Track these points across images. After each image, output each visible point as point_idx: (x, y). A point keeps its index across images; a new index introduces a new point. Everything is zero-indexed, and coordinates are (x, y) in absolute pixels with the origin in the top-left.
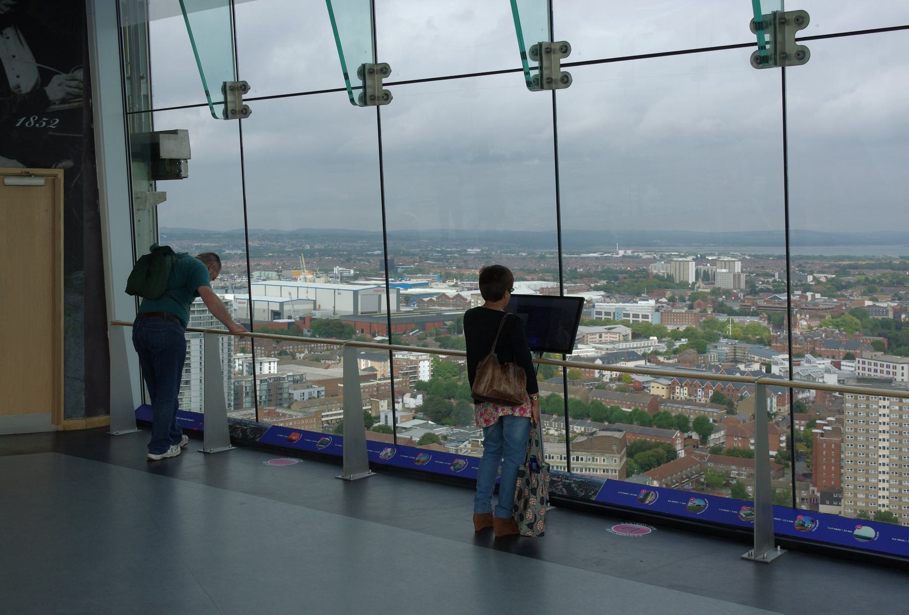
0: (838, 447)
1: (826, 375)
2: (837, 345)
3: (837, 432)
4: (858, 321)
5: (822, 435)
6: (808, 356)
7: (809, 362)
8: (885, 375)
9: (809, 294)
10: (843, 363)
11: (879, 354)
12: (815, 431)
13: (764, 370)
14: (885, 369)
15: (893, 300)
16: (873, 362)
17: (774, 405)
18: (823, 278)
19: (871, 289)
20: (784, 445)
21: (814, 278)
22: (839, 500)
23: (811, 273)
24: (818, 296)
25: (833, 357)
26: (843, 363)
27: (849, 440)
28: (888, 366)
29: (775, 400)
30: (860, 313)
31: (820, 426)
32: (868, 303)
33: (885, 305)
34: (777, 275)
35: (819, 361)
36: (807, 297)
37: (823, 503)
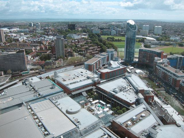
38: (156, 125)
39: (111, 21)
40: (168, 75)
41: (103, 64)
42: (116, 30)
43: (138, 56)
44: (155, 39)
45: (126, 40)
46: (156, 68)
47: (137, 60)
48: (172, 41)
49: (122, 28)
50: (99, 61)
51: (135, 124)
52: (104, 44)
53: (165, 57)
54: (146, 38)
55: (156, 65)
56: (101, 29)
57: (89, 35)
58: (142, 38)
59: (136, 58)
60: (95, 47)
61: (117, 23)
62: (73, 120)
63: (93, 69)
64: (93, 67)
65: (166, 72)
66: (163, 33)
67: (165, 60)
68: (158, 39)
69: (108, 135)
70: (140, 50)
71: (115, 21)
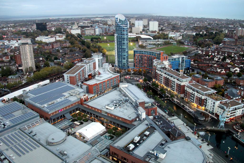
0: (20, 57)
1: (16, 44)
2: (17, 38)
3: (20, 54)
4: (20, 33)
5: (17, 55)
6: (12, 40)
7: (12, 41)
8: (26, 42)
9: (9, 28)
10: (18, 41)
11: (25, 38)
12: (15, 54)
13: (3, 44)
14: (26, 41)
15: (26, 28)
16: (24, 40)
17: (6, 51)
18: (11, 25)
19: (21, 26)
20: (10, 58)
21: (10, 25)
22: (22, 66)
23: (9, 24)
24: (11, 28)
25: (16, 40)
26: (18, 41)
27: (22, 55)
28: (27, 40)
29: (6, 50)
30: (20, 31)
31: (16, 53)
32: (21, 29)
33: (24, 29)
34: (2, 25)
35: (14, 41)
36: (9, 29)
37: (19, 67)
38: (164, 142)
39: (95, 16)
40: (171, 80)
41: (89, 74)
42: (101, 28)
43: (133, 60)
44: (151, 38)
45: (116, 40)
46: (156, 73)
48: (171, 38)
49: (110, 26)
50: (83, 70)
51: (138, 146)
52: (89, 47)
53: (166, 59)
54: (140, 37)
56: (82, 27)
58: (135, 36)
61: (103, 19)
62: (57, 153)
65: (168, 77)
66: (159, 30)
67: (166, 63)
70: (134, 51)
71: (99, 16)
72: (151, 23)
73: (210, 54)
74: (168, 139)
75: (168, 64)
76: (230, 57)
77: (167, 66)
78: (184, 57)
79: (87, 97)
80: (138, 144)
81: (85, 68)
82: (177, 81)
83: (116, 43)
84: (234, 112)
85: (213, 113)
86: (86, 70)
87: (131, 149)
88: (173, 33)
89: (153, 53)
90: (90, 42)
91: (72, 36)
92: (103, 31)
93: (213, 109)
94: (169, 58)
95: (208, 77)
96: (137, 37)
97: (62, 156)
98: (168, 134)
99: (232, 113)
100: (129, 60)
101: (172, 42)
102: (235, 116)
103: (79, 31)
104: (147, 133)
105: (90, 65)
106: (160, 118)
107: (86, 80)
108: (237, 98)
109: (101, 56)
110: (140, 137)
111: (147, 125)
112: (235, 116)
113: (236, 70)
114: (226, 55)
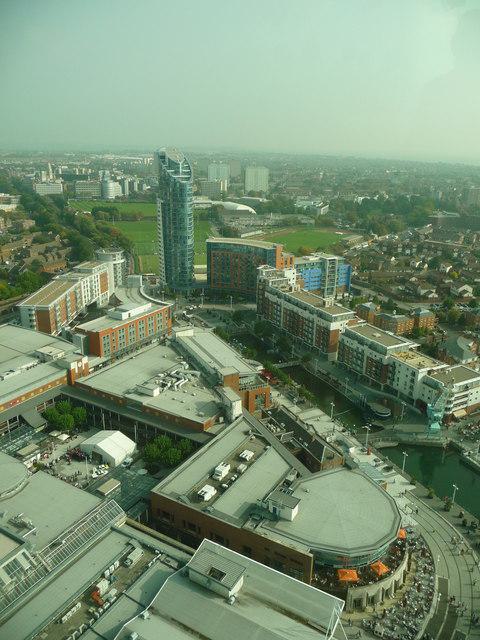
38: (291, 478)
44: (251, 209)
45: (160, 214)
46: (266, 300)
47: (203, 277)
48: (300, 211)
52: (87, 233)
53: (288, 263)
55: (264, 290)
57: (23, 201)
58: (209, 206)
59: (200, 272)
60: (50, 245)
63: (56, 323)
64: (55, 315)
65: (296, 309)
68: (258, 207)
69: (144, 546)
72: (250, 172)
73: (400, 250)
74: (303, 469)
75: (295, 276)
76: (447, 256)
77: (292, 282)
78: (336, 258)
79: (86, 365)
80: (224, 485)
81: (80, 287)
82: (320, 319)
83: (161, 223)
84: (466, 396)
85: (410, 401)
86: (80, 292)
87: (207, 497)
88: (306, 198)
89: (257, 248)
90: (91, 219)
91: (37, 198)
92: (123, 192)
93: (411, 387)
94: (298, 261)
95: (396, 308)
96: (214, 208)
97: (18, 532)
98: (302, 457)
99: (457, 398)
100: (196, 267)
101: (303, 222)
102: (465, 406)
103: (58, 187)
104: (248, 455)
105: (91, 281)
106: (279, 417)
107: (81, 318)
108: (470, 360)
109: (120, 256)
110: (228, 468)
111: (247, 433)
112: (465, 406)
113: (465, 291)
114: (439, 253)
